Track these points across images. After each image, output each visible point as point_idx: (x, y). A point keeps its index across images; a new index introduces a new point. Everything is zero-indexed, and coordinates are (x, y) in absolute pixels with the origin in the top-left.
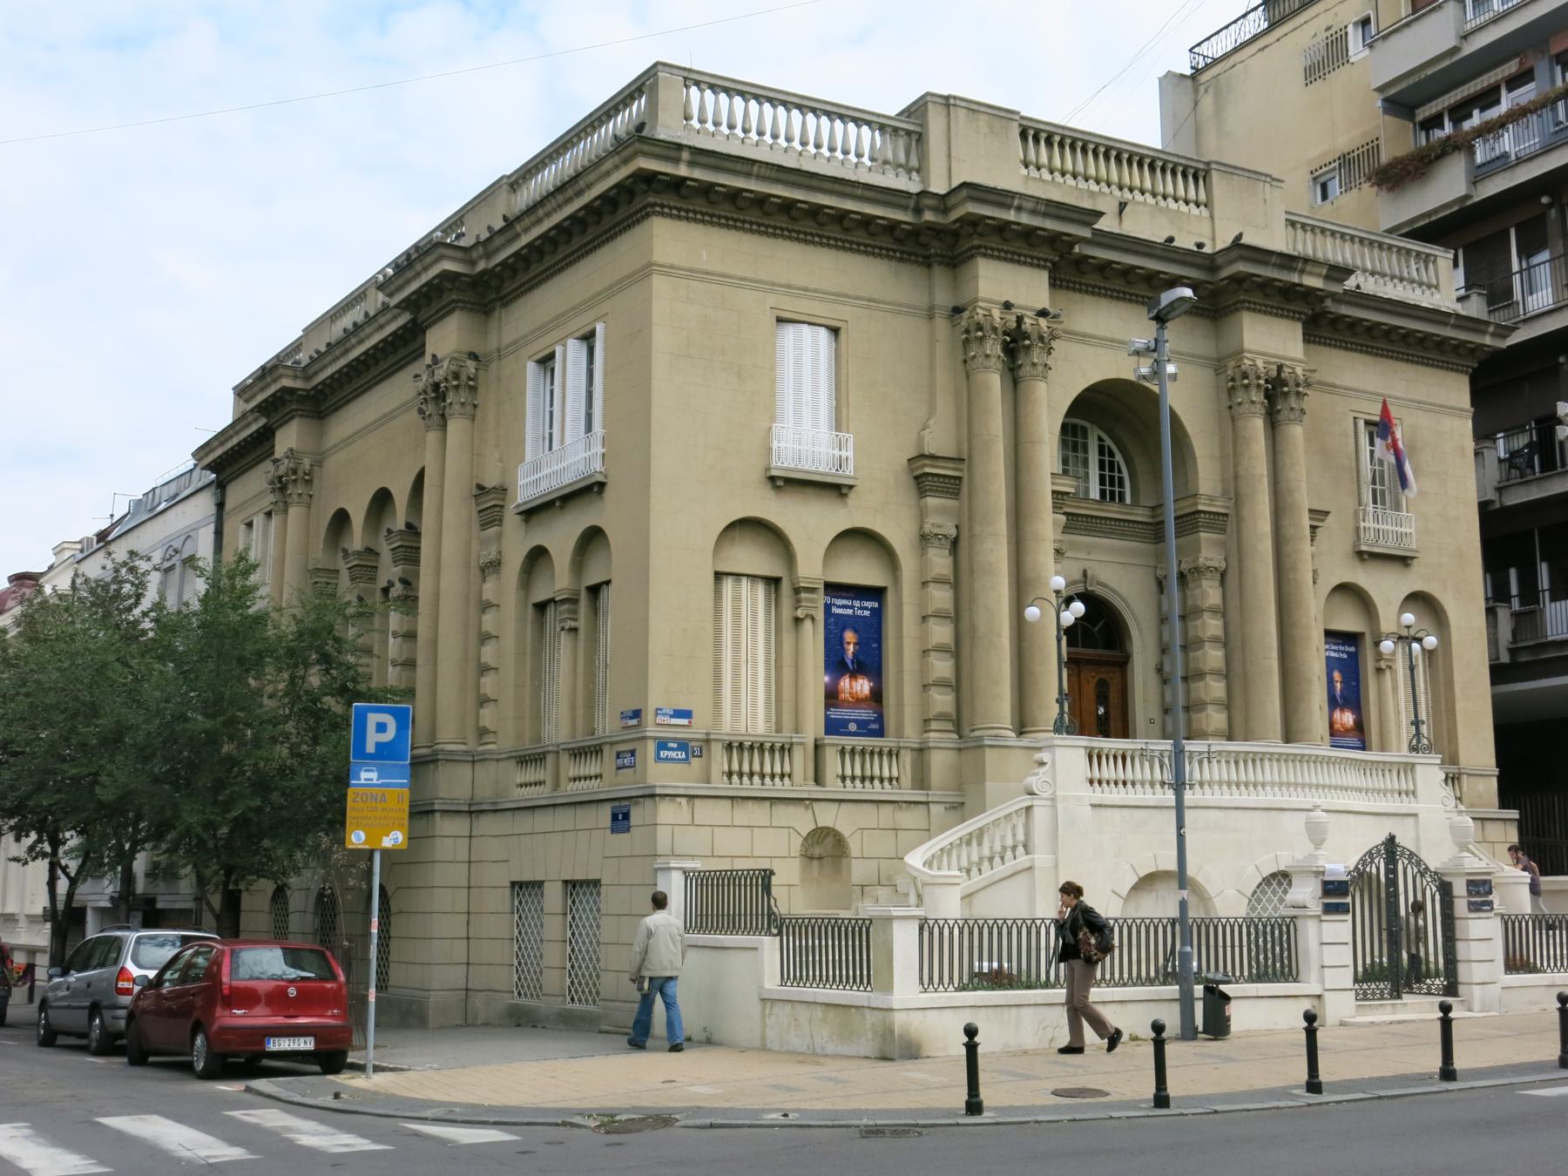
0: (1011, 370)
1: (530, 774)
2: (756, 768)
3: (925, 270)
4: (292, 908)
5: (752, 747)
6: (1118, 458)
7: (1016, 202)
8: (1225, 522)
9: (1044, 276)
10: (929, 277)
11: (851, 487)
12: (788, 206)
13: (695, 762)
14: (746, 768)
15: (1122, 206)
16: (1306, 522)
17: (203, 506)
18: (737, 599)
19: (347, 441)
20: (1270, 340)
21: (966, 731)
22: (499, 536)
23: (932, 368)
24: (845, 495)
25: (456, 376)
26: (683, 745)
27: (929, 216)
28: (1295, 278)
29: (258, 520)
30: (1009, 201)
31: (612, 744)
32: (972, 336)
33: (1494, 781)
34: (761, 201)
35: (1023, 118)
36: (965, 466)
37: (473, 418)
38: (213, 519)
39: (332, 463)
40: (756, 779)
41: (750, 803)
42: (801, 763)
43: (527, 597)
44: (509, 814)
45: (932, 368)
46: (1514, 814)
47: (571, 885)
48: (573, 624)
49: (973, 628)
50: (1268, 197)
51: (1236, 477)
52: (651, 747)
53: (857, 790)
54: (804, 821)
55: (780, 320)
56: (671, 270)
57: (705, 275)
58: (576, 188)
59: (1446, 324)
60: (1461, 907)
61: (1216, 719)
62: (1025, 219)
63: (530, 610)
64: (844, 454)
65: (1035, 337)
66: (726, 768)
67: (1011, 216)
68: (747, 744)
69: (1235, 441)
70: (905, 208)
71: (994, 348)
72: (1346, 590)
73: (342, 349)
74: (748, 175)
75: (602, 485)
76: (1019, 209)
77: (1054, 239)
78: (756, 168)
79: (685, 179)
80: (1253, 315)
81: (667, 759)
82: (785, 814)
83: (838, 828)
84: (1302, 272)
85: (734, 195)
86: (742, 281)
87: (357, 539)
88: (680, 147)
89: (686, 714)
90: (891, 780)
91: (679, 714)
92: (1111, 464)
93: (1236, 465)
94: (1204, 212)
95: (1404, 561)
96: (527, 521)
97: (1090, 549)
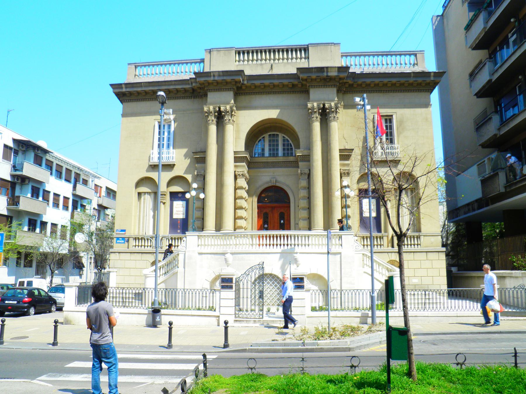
5: (142, 239)
6: (291, 142)
7: (212, 74)
18: (144, 199)
26: (123, 238)
27: (194, 85)
41: (136, 254)
46: (444, 249)
52: (115, 239)
70: (189, 84)
71: (212, 118)
81: (119, 243)
88: (121, 84)
89: (124, 231)
91: (122, 231)
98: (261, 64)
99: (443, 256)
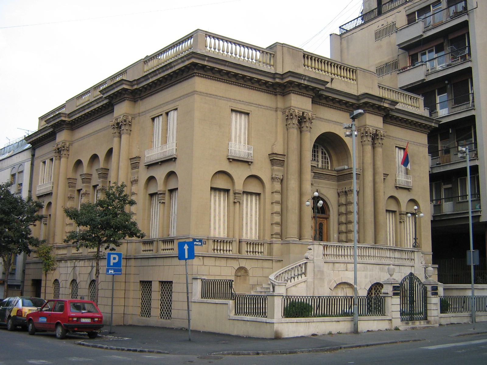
0: (300, 128)
1: (147, 247)
2: (222, 248)
3: (275, 97)
4: (61, 286)
9: (310, 100)
10: (276, 98)
11: (252, 162)
12: (236, 75)
13: (204, 245)
14: (219, 248)
15: (332, 79)
16: (383, 178)
17: (27, 155)
19: (83, 138)
20: (374, 122)
21: (284, 239)
22: (138, 172)
23: (276, 126)
24: (250, 165)
25: (125, 121)
27: (277, 80)
29: (48, 161)
30: (302, 77)
31: (177, 239)
32: (289, 117)
33: (431, 256)
34: (228, 73)
35: (304, 51)
36: (286, 157)
37: (130, 134)
38: (30, 159)
39: (76, 145)
40: (222, 251)
43: (146, 192)
44: (140, 260)
45: (276, 126)
46: (437, 266)
47: (162, 283)
48: (163, 201)
49: (287, 207)
51: (363, 163)
53: (251, 255)
54: (236, 265)
55: (232, 110)
56: (200, 93)
57: (210, 95)
58: (171, 66)
60: (429, 294)
61: (354, 236)
62: (306, 83)
63: (148, 196)
64: (250, 152)
65: (307, 118)
66: (213, 248)
67: (302, 82)
68: (219, 241)
69: (363, 152)
71: (295, 121)
72: (392, 197)
73: (83, 109)
74: (225, 65)
75: (175, 158)
76: (305, 80)
77: (314, 89)
78: (227, 64)
79: (206, 66)
80: (369, 114)
83: (246, 267)
84: (384, 102)
85: (220, 71)
86: (221, 98)
87: (85, 169)
90: (261, 252)
92: (325, 157)
93: (363, 160)
94: (355, 83)
95: (408, 189)
96: (148, 168)
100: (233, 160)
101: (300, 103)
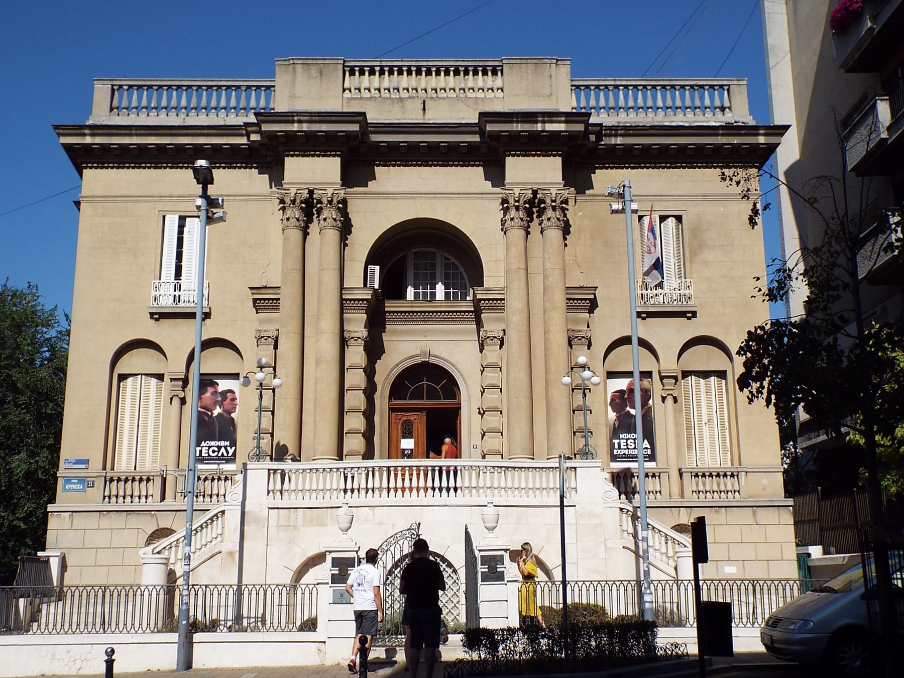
8: (497, 305)
20: (540, 172)
26: (81, 480)
28: (539, 127)
33: (780, 478)
42: (155, 489)
46: (790, 502)
50: (553, 74)
59: (718, 135)
67: (295, 127)
70: (241, 135)
76: (300, 122)
82: (134, 520)
89: (86, 462)
97: (425, 333)
98: (401, 100)
99: (788, 518)
100: (160, 316)
101: (316, 172)
